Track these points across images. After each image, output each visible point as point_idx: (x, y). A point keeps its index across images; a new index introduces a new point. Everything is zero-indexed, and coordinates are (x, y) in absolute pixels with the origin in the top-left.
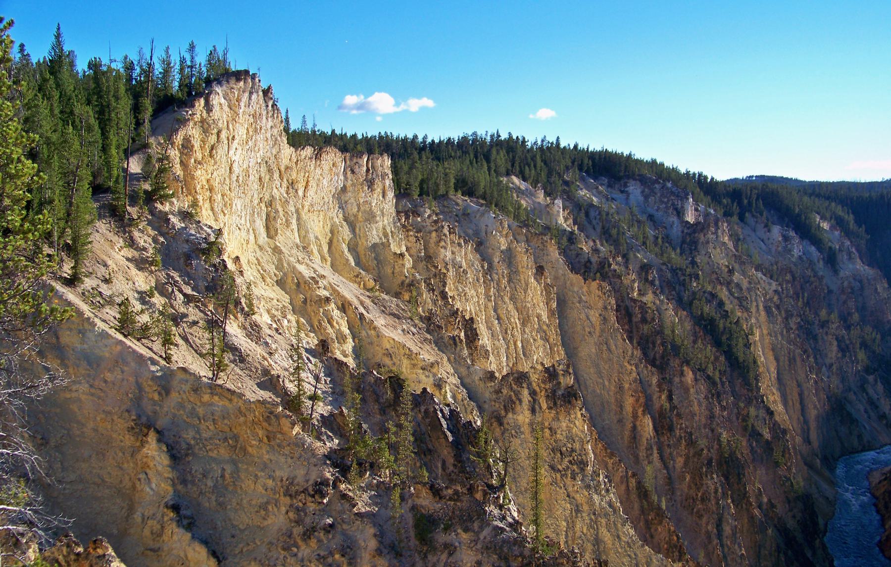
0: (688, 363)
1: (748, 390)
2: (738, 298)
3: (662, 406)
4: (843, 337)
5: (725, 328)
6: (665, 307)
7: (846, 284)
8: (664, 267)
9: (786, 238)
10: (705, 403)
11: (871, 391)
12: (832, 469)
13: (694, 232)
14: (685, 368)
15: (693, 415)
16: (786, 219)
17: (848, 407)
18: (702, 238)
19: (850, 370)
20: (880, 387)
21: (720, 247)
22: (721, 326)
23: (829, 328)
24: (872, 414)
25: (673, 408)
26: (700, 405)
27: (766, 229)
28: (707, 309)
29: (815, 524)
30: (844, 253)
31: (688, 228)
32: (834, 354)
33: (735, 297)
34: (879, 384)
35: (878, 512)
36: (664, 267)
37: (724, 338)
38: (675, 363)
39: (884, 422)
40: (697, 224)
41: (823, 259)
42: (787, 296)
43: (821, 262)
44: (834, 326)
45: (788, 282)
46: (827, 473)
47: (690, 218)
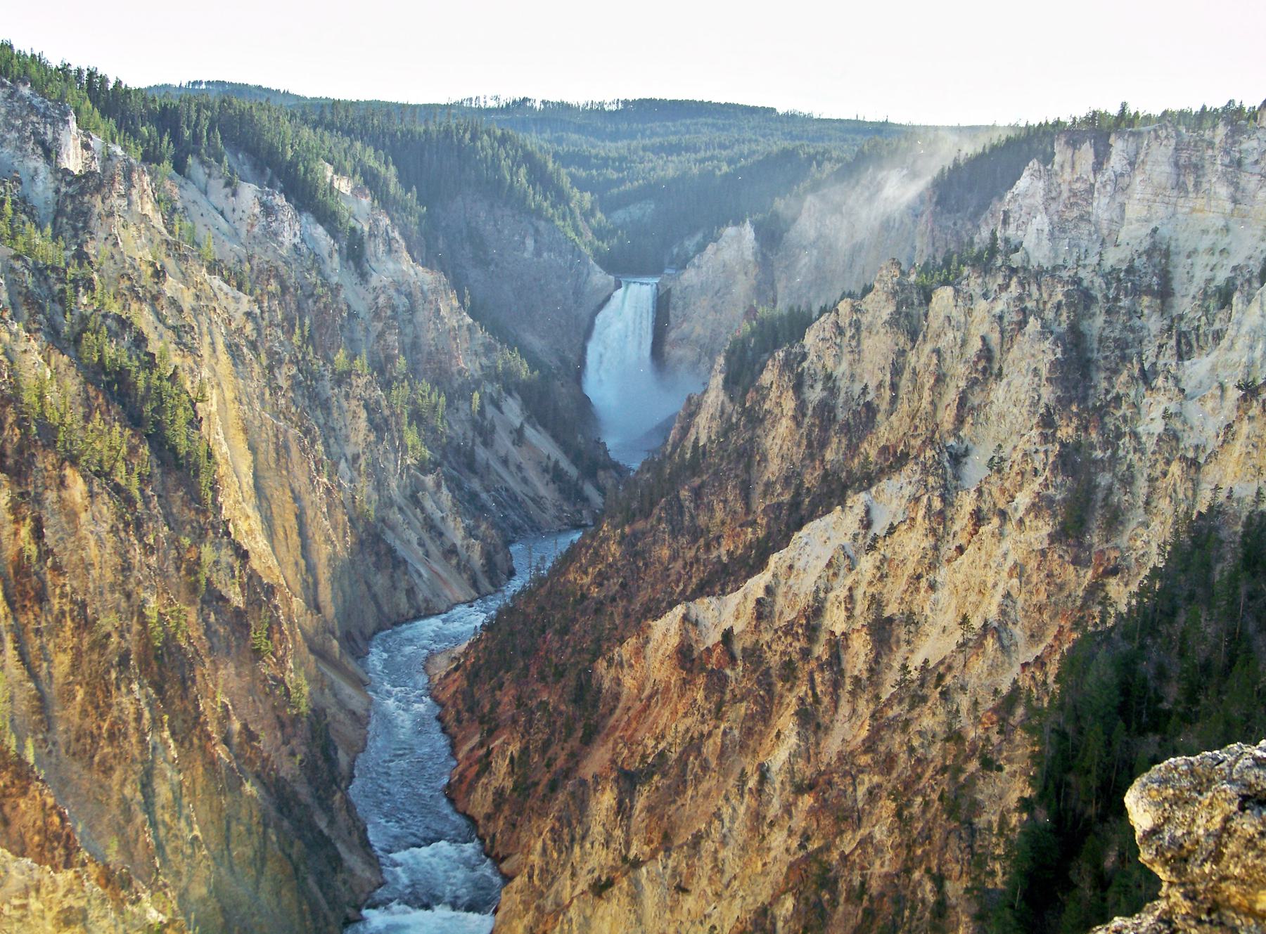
0: (74, 461)
1: (197, 510)
2: (174, 328)
3: (21, 551)
4: (377, 402)
5: (148, 388)
6: (23, 346)
7: (381, 300)
8: (18, 264)
9: (268, 210)
10: (110, 541)
11: (429, 504)
12: (360, 655)
13: (82, 192)
14: (68, 472)
15: (88, 566)
16: (268, 171)
17: (390, 537)
18: (99, 207)
20: (446, 495)
21: (132, 228)
22: (141, 384)
23: (351, 385)
24: (433, 548)
25: (45, 553)
26: (100, 543)
27: (228, 190)
28: (110, 351)
29: (331, 761)
30: (379, 241)
31: (69, 184)
32: (361, 437)
33: (169, 328)
34: (444, 490)
35: (444, 730)
36: (18, 264)
37: (148, 408)
38: (45, 461)
39: (454, 562)
40: (89, 175)
41: (340, 251)
42: (271, 324)
43: (336, 256)
44: (362, 381)
45: (272, 296)
46: (352, 665)
47: (73, 160)
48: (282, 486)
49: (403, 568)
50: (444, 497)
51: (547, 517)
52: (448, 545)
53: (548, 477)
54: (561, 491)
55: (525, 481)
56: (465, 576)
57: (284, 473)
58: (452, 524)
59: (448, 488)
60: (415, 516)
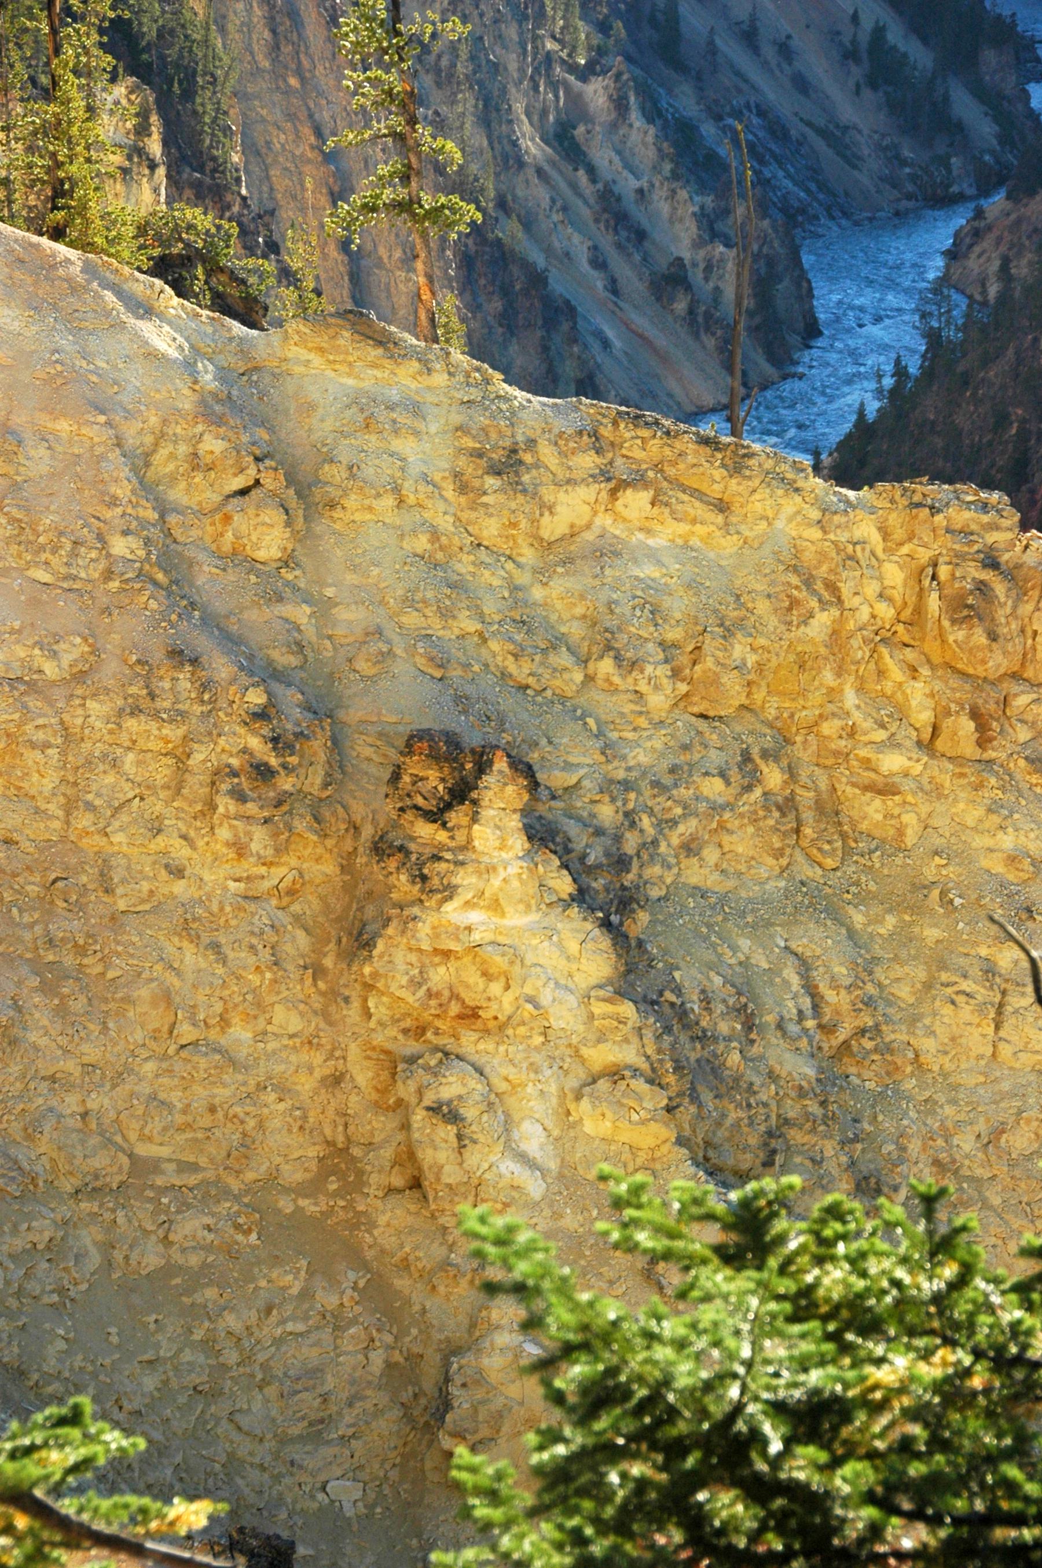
19: (513, 66)
24: (624, 271)
34: (635, 117)
39: (681, 306)
48: (291, 117)
49: (565, 326)
50: (635, 137)
51: (864, 179)
52: (662, 264)
53: (857, 72)
54: (894, 107)
55: (802, 85)
56: (710, 342)
57: (293, 82)
58: (665, 208)
59: (643, 109)
60: (574, 186)
